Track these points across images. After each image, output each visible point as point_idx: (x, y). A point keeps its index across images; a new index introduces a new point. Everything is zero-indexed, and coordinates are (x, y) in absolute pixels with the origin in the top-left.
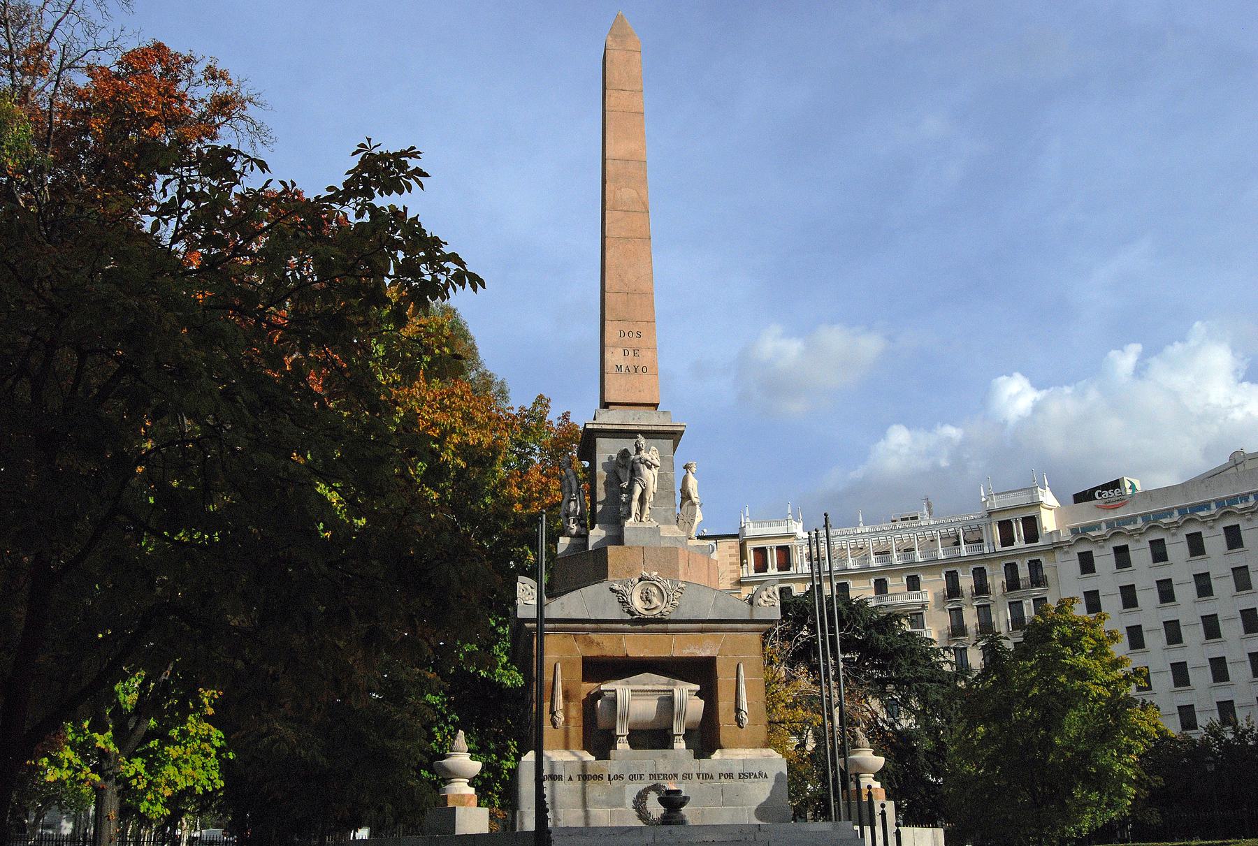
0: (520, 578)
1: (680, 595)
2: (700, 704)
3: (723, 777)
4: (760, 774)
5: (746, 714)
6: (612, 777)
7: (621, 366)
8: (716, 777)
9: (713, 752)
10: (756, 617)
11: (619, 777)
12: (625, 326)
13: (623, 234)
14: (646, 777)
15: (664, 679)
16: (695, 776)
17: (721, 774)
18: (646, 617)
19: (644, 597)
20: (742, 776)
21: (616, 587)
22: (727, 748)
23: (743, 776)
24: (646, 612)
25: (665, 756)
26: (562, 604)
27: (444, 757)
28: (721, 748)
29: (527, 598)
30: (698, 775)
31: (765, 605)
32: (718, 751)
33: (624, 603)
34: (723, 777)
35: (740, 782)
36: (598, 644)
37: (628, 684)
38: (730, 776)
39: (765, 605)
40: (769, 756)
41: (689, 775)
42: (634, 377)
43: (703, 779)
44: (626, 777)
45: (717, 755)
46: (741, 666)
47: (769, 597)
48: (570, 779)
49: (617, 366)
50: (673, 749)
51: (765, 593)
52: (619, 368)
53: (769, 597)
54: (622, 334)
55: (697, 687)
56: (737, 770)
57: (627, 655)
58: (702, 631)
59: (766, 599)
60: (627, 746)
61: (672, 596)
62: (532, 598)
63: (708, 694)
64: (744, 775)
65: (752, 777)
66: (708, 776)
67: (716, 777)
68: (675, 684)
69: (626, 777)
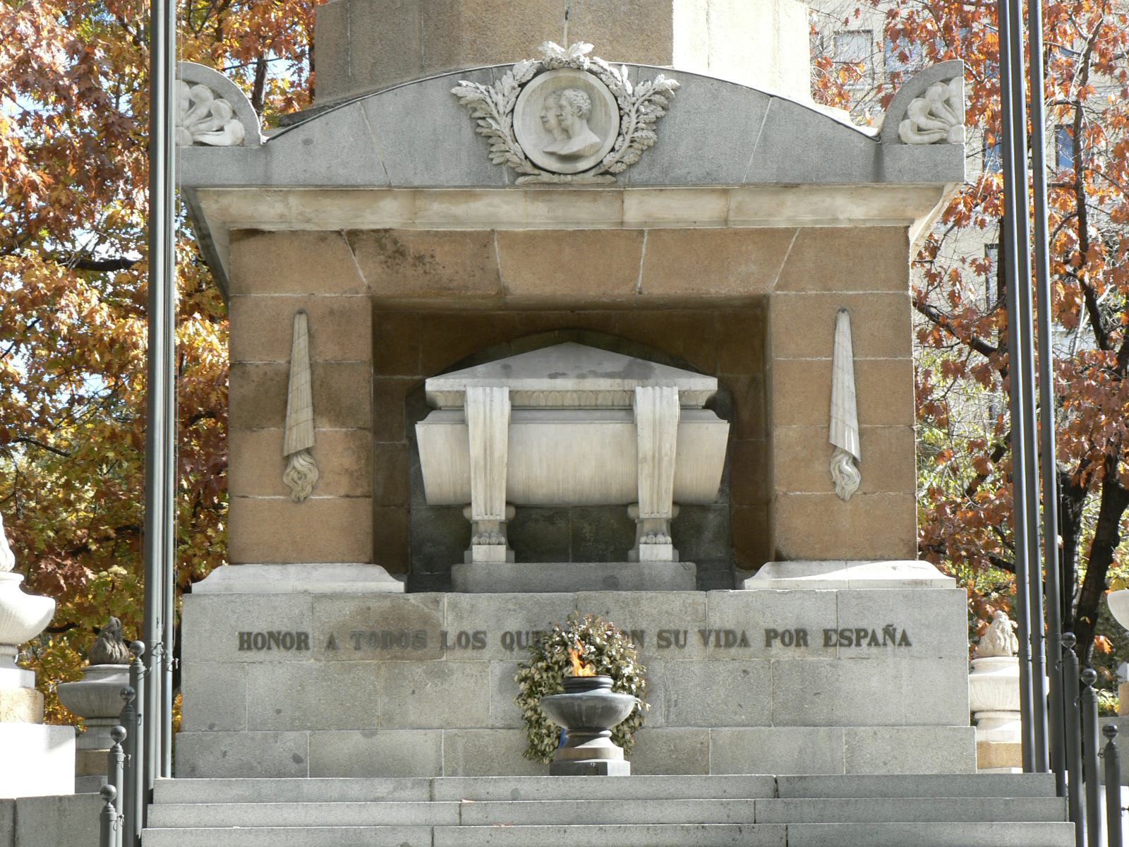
1: (661, 113)
3: (777, 643)
4: (889, 631)
5: (855, 462)
6: (451, 640)
9: (754, 568)
15: (620, 361)
16: (694, 639)
17: (771, 635)
18: (555, 179)
19: (553, 121)
20: (834, 638)
21: (467, 89)
25: (612, 584)
26: (307, 142)
28: (779, 558)
29: (203, 126)
30: (704, 635)
31: (917, 138)
32: (766, 568)
33: (488, 139)
34: (777, 643)
35: (825, 658)
36: (420, 258)
37: (508, 372)
38: (799, 637)
39: (917, 138)
40: (917, 583)
41: (677, 633)
43: (718, 645)
44: (493, 640)
45: (762, 581)
46: (844, 324)
47: (932, 114)
48: (331, 644)
50: (637, 560)
51: (916, 105)
53: (932, 114)
55: (707, 385)
56: (817, 619)
57: (503, 291)
59: (923, 121)
60: (501, 552)
61: (633, 115)
62: (216, 123)
64: (842, 634)
65: (865, 642)
66: (731, 639)
67: (757, 639)
68: (644, 378)
69: (493, 640)
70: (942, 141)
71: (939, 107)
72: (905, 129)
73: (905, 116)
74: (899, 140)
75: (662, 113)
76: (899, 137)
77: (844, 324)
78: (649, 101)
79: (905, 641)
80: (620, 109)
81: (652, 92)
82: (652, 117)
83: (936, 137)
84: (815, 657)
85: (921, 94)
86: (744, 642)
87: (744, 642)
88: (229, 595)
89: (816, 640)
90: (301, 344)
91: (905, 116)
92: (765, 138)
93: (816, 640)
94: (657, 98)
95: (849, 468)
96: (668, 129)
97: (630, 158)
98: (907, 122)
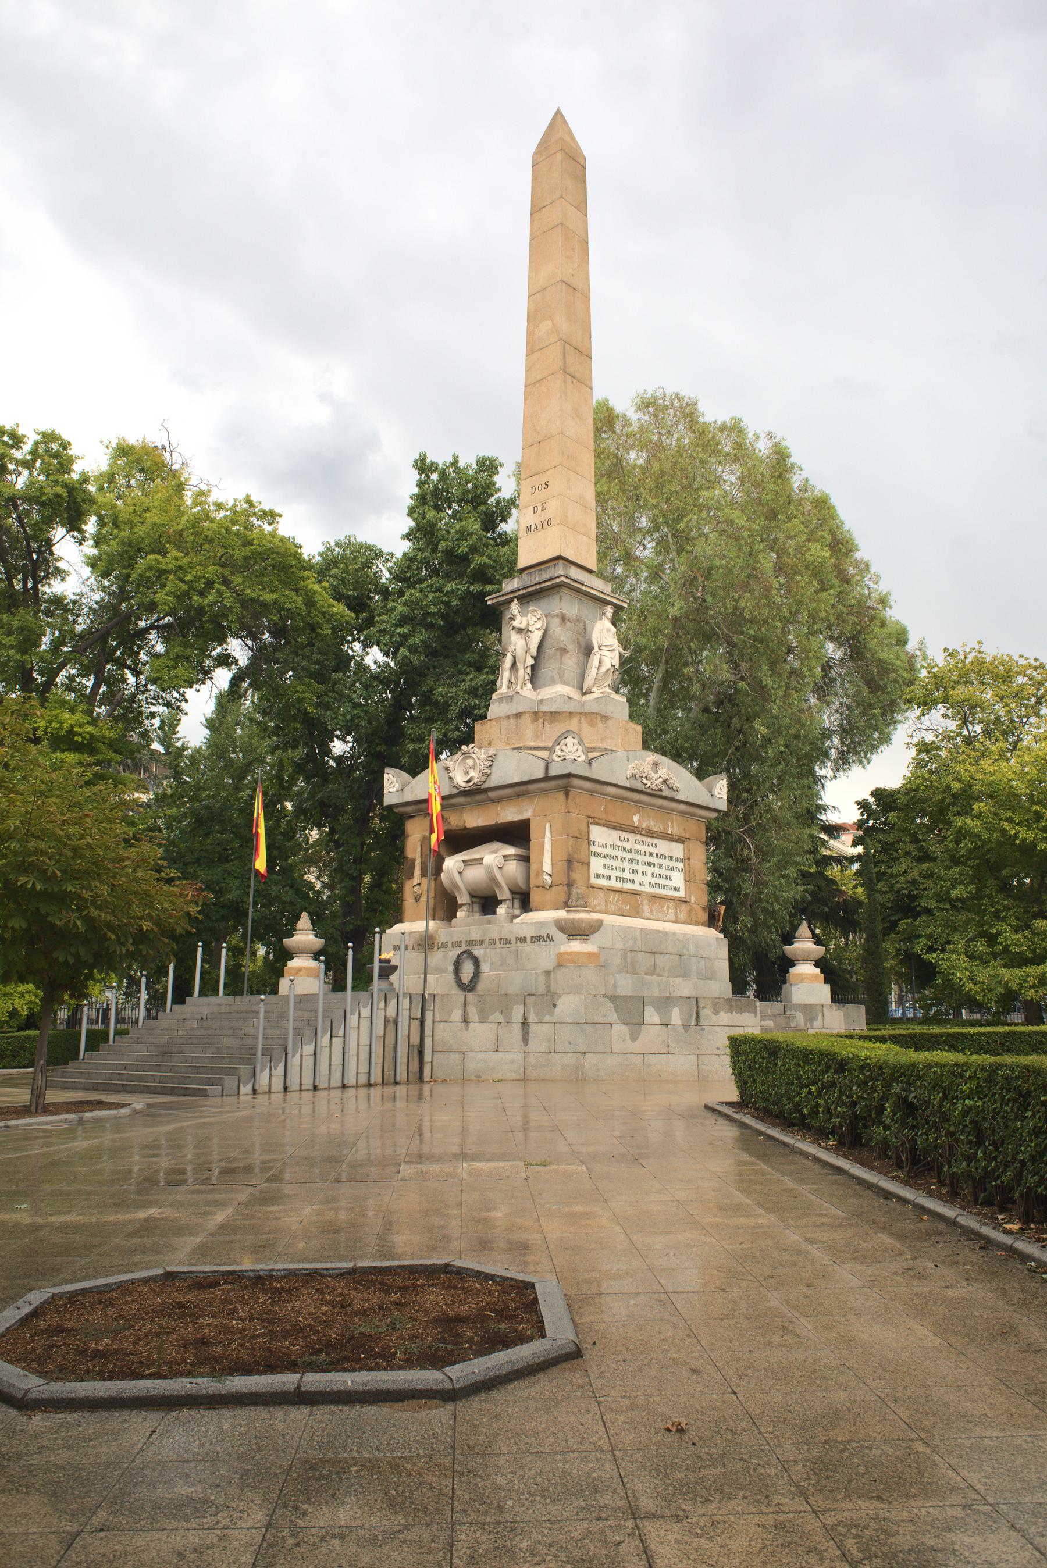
0: (387, 770)
2: (513, 868)
4: (548, 936)
8: (513, 941)
10: (553, 772)
11: (444, 945)
12: (536, 481)
13: (539, 377)
14: (463, 945)
16: (498, 942)
17: (517, 939)
22: (536, 910)
23: (537, 939)
24: (464, 785)
27: (293, 936)
34: (519, 944)
38: (523, 940)
42: (541, 533)
44: (450, 944)
52: (529, 529)
54: (533, 490)
56: (529, 933)
57: (466, 828)
58: (519, 796)
59: (559, 753)
63: (525, 859)
67: (513, 941)
69: (450, 944)
71: (564, 748)
72: (554, 757)
77: (548, 826)
79: (552, 940)
84: (528, 948)
86: (510, 942)
87: (510, 942)
88: (391, 935)
89: (529, 940)
90: (419, 850)
93: (529, 940)
95: (546, 877)
96: (494, 768)
97: (483, 779)
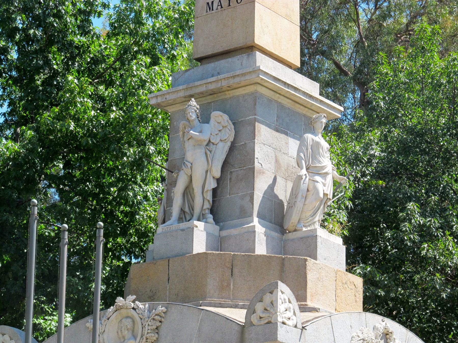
7: (213, 2)
49: (208, 3)
70: (269, 323)
72: (254, 319)
73: (254, 312)
74: (252, 324)
75: (160, 324)
76: (252, 322)
78: (154, 319)
80: (142, 324)
81: (154, 315)
82: (154, 327)
83: (266, 321)
85: (261, 301)
91: (254, 312)
92: (199, 330)
94: (157, 317)
96: (163, 331)
98: (255, 314)
